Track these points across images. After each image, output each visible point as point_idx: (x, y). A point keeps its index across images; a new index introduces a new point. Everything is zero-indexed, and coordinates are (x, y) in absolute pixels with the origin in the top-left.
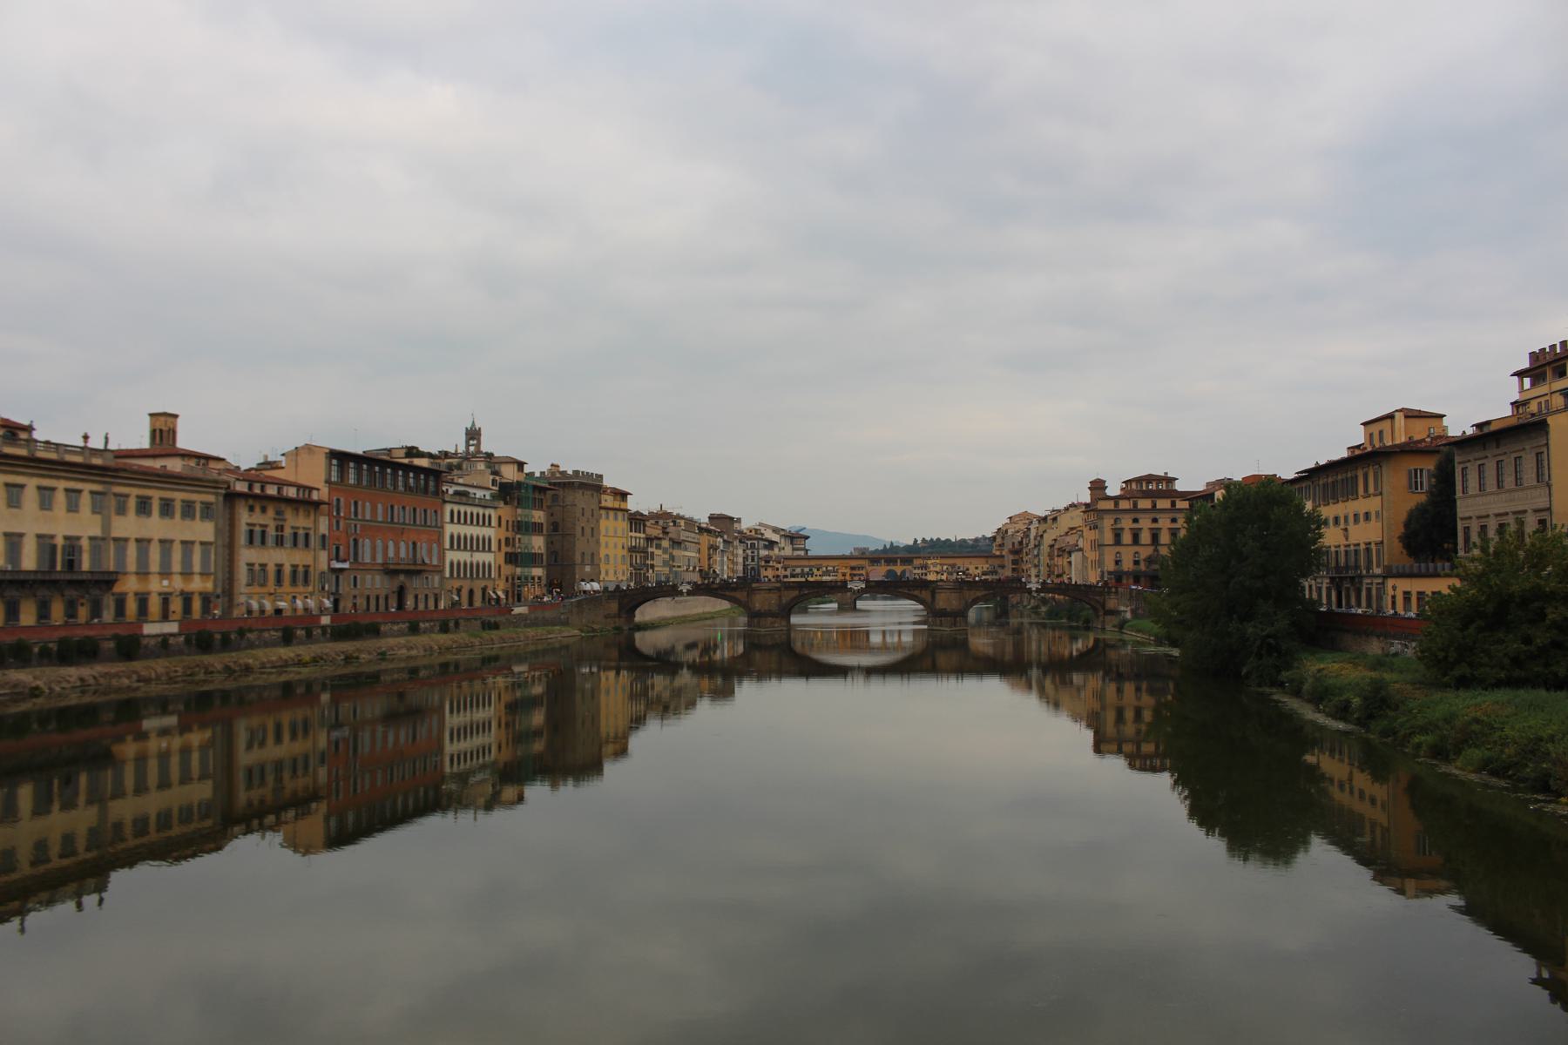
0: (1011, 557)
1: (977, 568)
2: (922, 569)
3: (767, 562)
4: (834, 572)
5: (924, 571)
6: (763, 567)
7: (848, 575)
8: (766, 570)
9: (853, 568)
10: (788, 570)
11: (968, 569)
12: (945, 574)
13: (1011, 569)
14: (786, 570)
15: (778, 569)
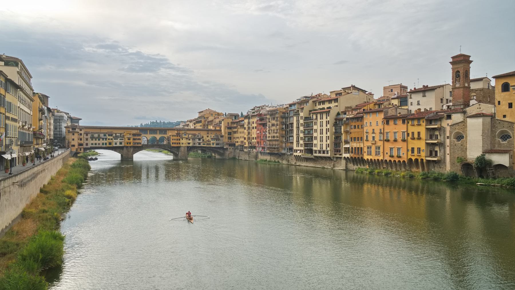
0: (228, 131)
1: (208, 137)
2: (177, 136)
3: (75, 129)
4: (121, 137)
5: (178, 138)
6: (71, 132)
7: (132, 139)
8: (73, 134)
9: (134, 135)
10: (89, 135)
11: (203, 137)
12: (191, 140)
13: (227, 138)
14: (87, 135)
15: (81, 134)
